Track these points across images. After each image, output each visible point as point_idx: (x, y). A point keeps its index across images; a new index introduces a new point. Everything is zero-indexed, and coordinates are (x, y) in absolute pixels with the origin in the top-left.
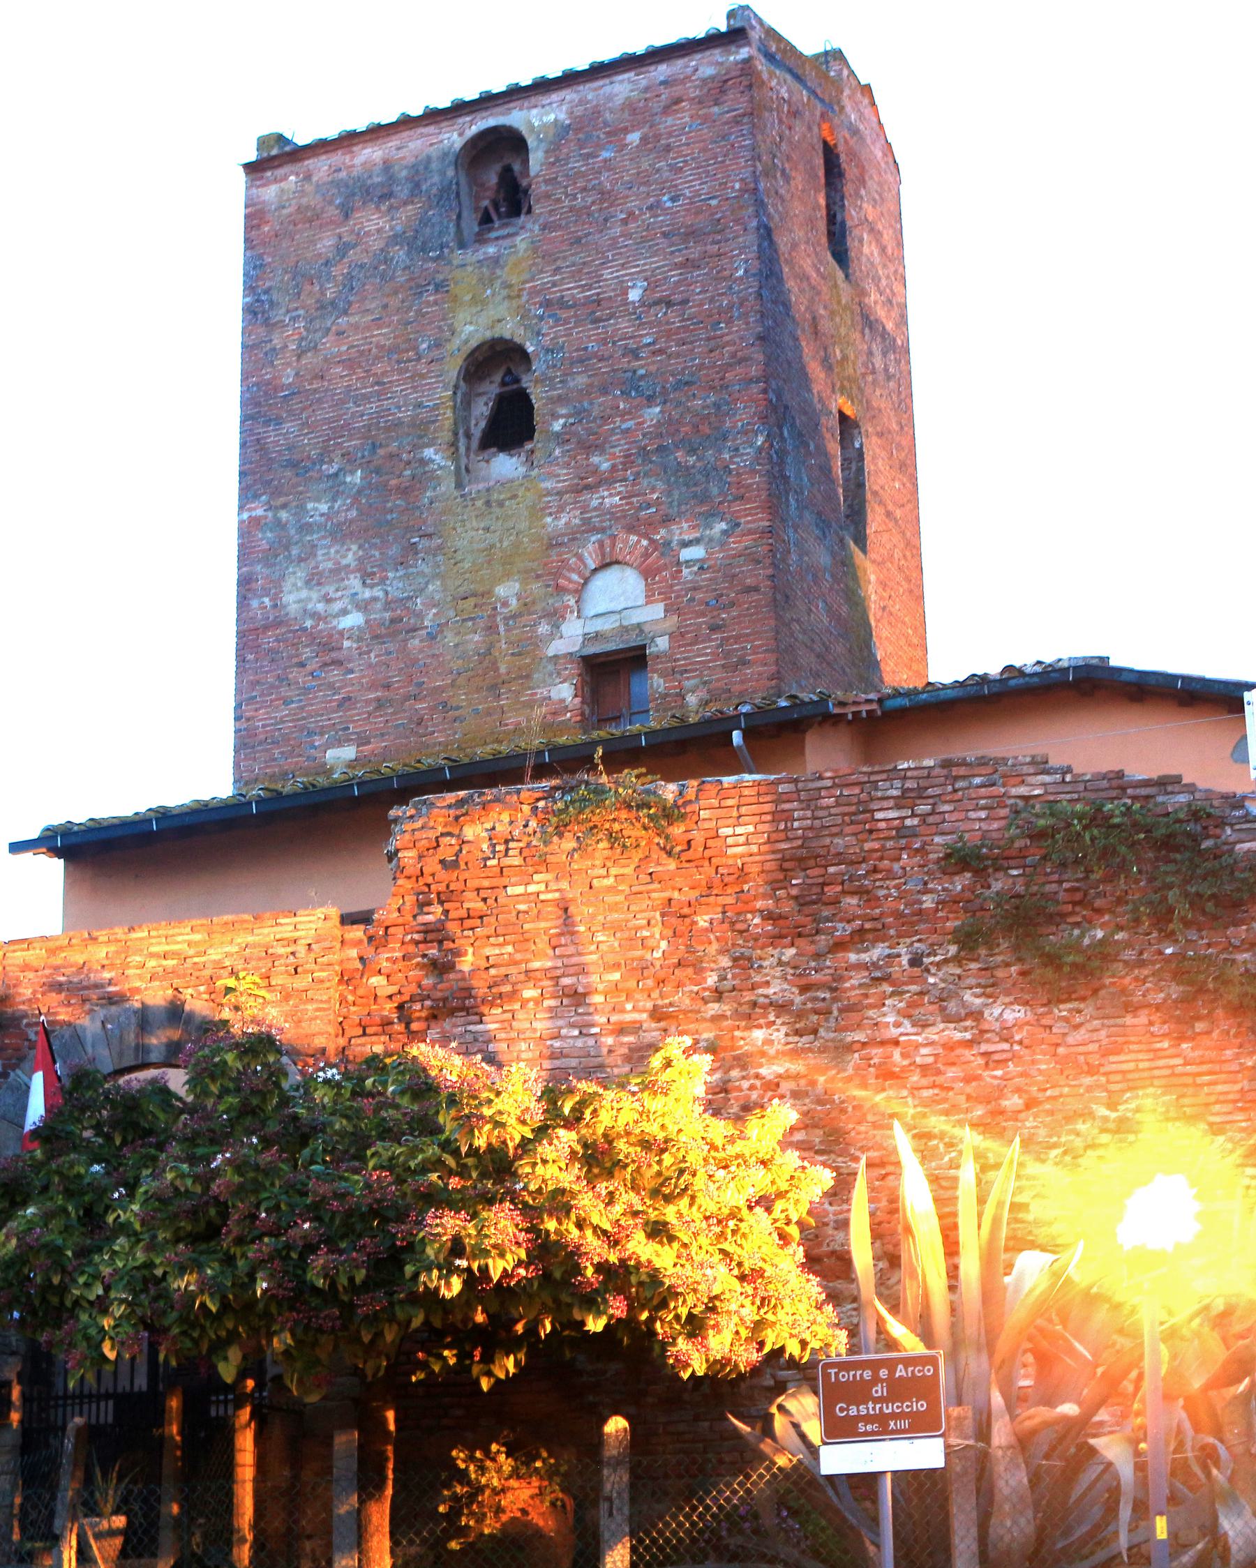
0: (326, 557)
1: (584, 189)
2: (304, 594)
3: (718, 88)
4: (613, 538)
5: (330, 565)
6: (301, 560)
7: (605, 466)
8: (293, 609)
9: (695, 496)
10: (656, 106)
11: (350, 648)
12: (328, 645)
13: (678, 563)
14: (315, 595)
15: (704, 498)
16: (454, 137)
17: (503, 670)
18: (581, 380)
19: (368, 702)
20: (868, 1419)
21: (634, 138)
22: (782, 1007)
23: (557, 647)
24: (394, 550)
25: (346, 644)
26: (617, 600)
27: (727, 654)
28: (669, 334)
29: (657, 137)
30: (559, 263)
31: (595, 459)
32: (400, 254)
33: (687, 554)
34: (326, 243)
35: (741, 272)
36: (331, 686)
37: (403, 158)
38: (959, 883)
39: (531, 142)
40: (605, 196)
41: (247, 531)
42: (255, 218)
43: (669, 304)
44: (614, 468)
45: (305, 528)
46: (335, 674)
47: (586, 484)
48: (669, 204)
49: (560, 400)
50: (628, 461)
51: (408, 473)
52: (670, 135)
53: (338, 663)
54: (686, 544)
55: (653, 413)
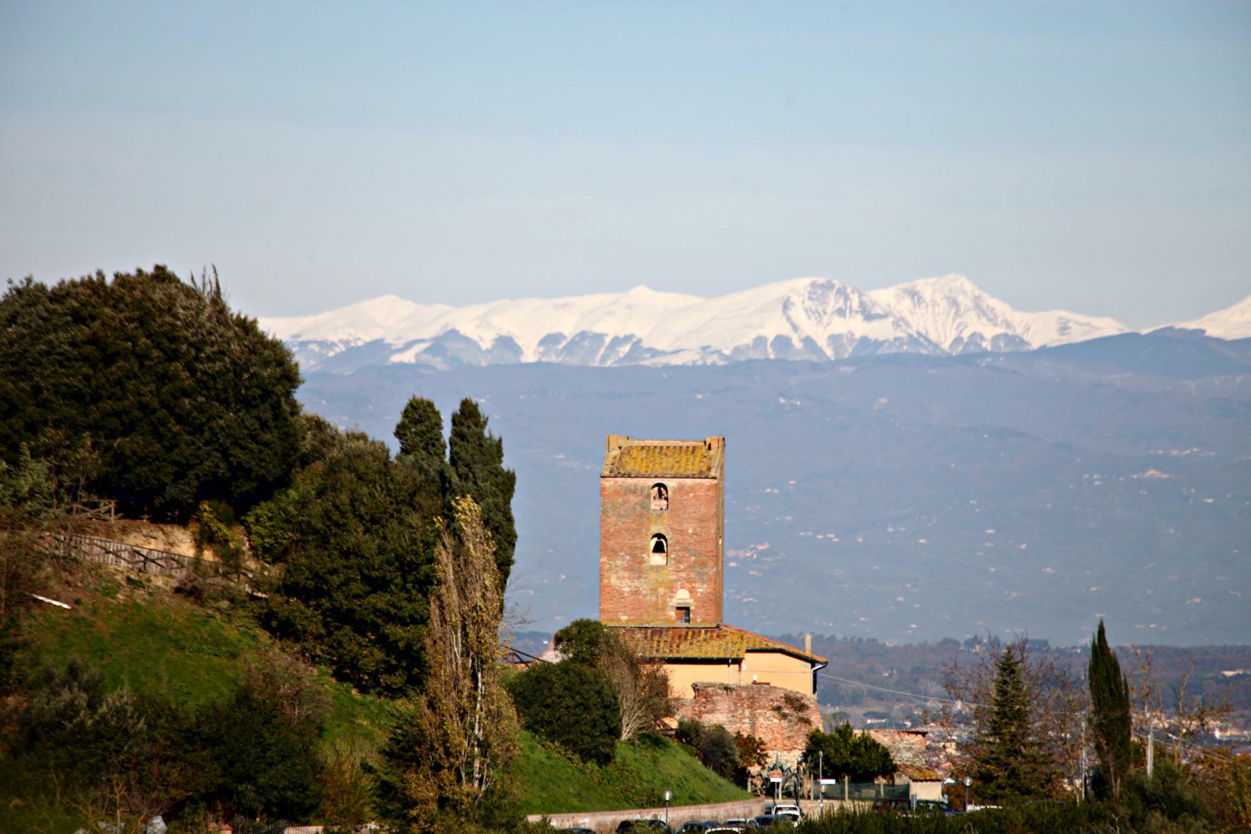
0: (621, 573)
3: (709, 488)
12: (621, 593)
18: (677, 548)
26: (683, 596)
32: (638, 508)
34: (620, 500)
55: (693, 559)
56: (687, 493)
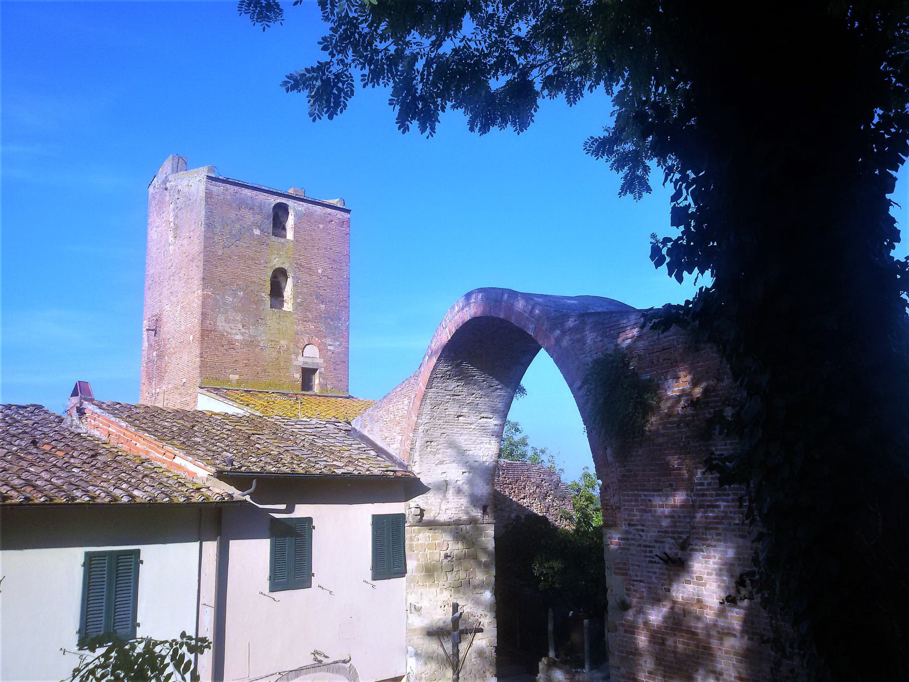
0: (231, 315)
2: (224, 324)
8: (220, 328)
12: (231, 343)
14: (227, 326)
16: (274, 200)
18: (305, 290)
21: (321, 226)
33: (329, 348)
41: (205, 298)
42: (209, 195)
46: (233, 352)
49: (300, 293)
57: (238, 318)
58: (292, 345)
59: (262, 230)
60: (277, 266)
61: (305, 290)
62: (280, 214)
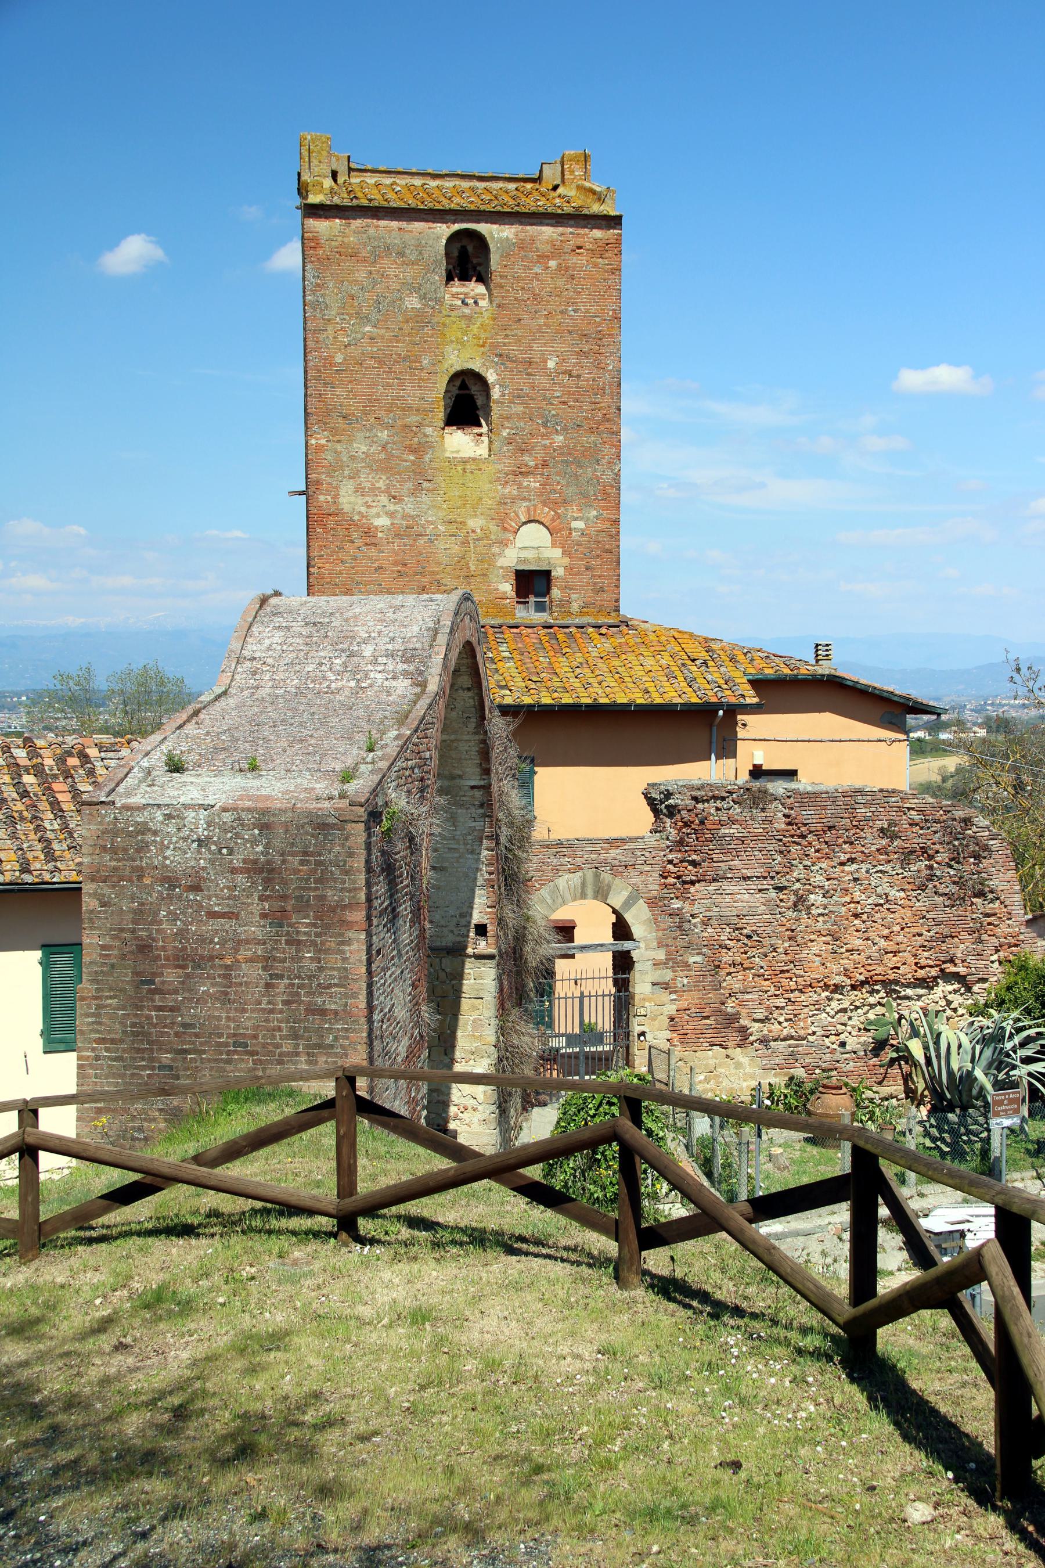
0: (366, 479)
1: (523, 288)
2: (353, 499)
4: (535, 506)
5: (369, 485)
6: (350, 478)
7: (532, 463)
8: (346, 508)
9: (580, 493)
10: (567, 248)
11: (381, 538)
12: (369, 532)
13: (570, 529)
14: (360, 500)
15: (585, 496)
16: (444, 230)
17: (473, 568)
18: (520, 409)
19: (393, 571)
20: (1002, 1111)
21: (553, 263)
22: (821, 887)
23: (501, 562)
24: (409, 485)
25: (380, 535)
27: (595, 584)
28: (569, 393)
29: (567, 269)
30: (508, 332)
31: (526, 458)
33: (575, 524)
35: (611, 367)
36: (370, 558)
37: (411, 232)
38: (884, 842)
39: (491, 246)
40: (536, 297)
43: (570, 376)
44: (536, 467)
45: (353, 458)
46: (372, 552)
47: (521, 472)
48: (572, 313)
50: (545, 464)
51: (416, 439)
52: (574, 268)
53: (374, 545)
54: (576, 519)
56: (543, 258)
57: (381, 484)
58: (493, 528)
59: (423, 297)
60: (458, 367)
61: (520, 409)
62: (470, 249)
